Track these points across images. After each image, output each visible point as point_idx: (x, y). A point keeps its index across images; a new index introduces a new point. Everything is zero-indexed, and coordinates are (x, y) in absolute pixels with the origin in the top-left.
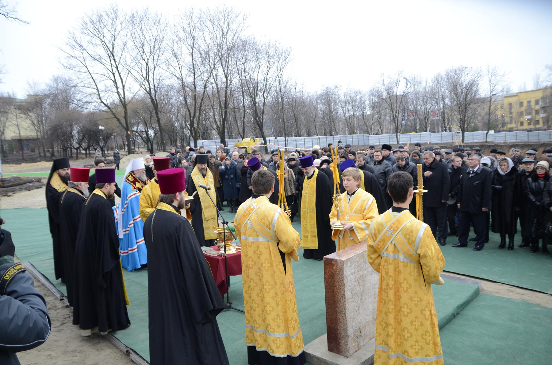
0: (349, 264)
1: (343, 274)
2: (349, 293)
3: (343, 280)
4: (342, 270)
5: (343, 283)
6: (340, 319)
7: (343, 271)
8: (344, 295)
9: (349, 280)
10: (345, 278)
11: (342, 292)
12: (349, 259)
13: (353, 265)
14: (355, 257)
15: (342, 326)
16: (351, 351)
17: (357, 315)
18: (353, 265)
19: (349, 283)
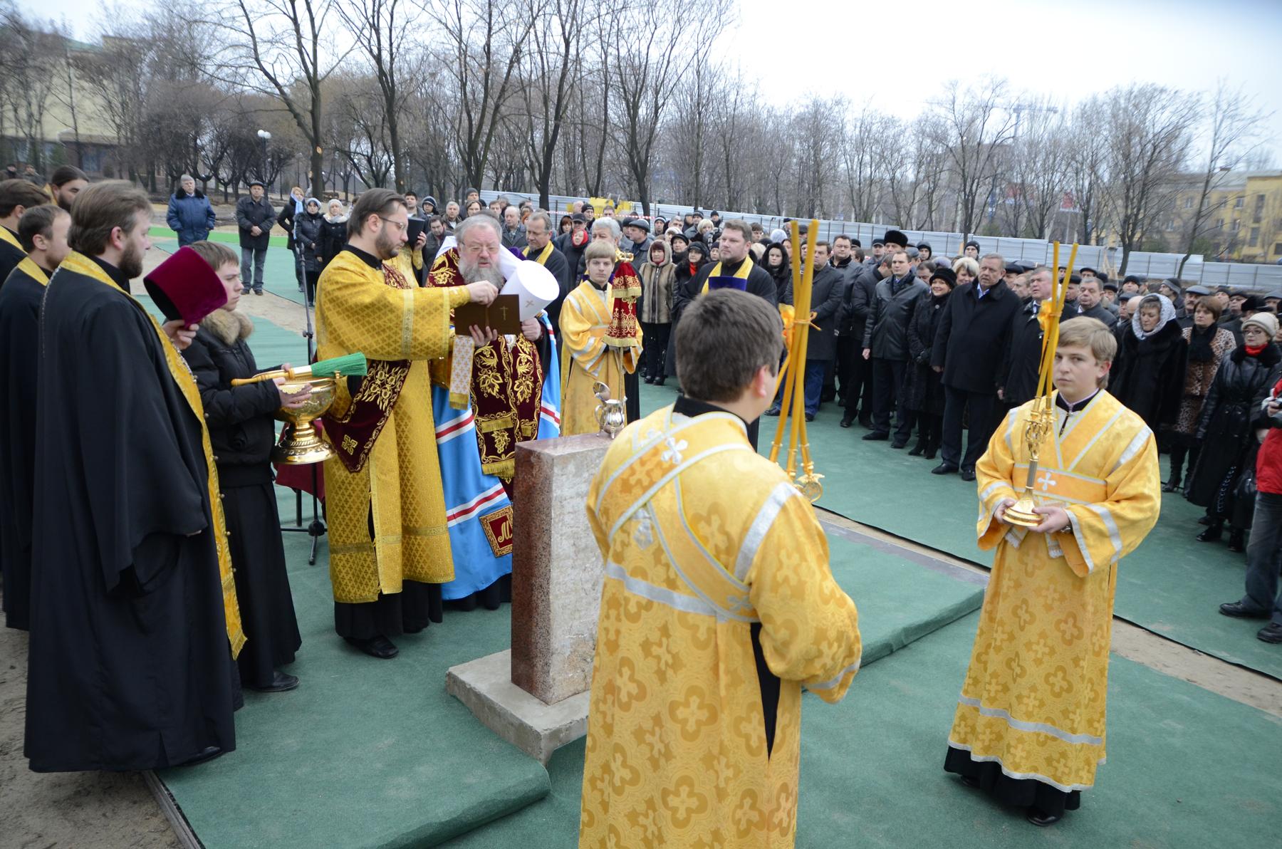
0: (571, 468)
1: (550, 491)
2: (565, 542)
3: (549, 508)
4: (548, 480)
5: (549, 515)
6: (537, 607)
7: (550, 484)
8: (549, 545)
9: (568, 508)
10: (554, 503)
11: (545, 539)
12: (573, 456)
13: (586, 475)
14: (596, 454)
15: (540, 624)
16: (557, 691)
17: (590, 604)
18: (586, 475)
19: (568, 519)
